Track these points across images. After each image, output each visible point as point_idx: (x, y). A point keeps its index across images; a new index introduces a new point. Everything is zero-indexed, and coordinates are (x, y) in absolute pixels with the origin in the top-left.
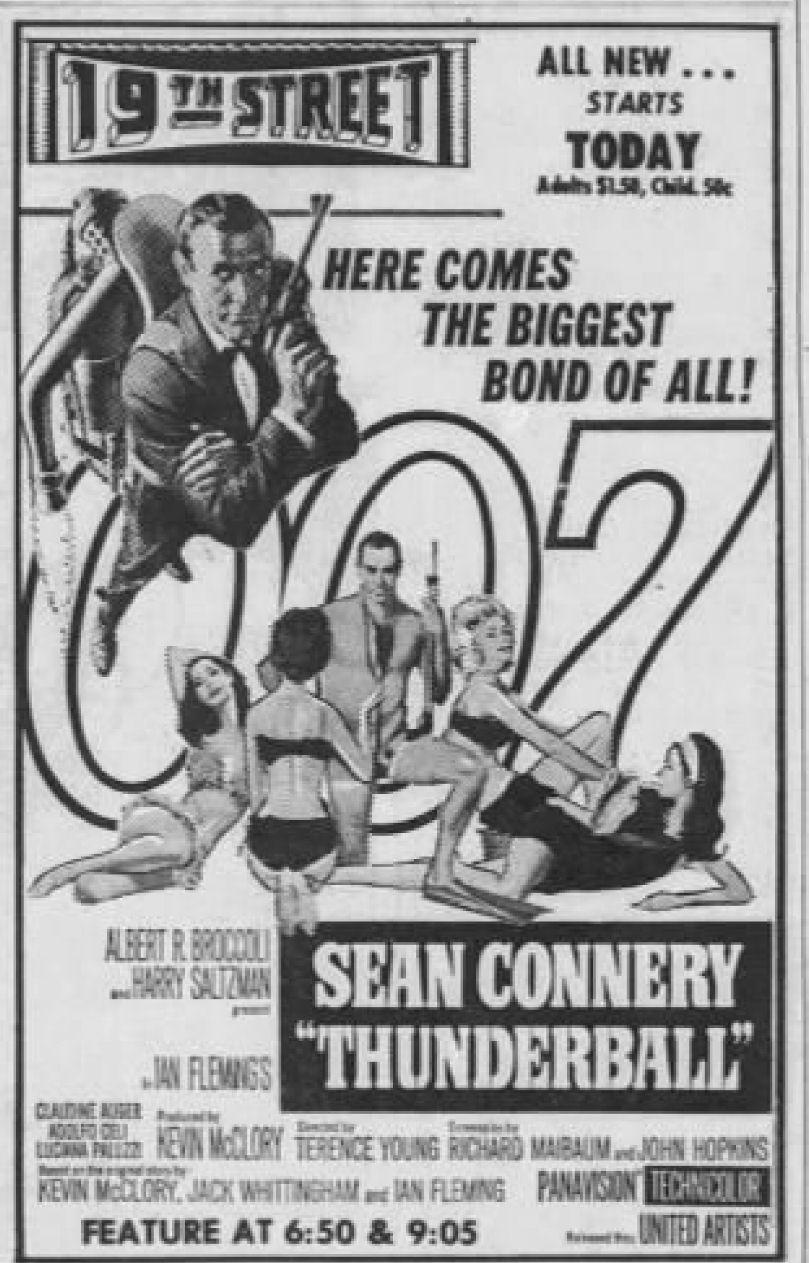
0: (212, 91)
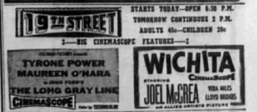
0: (61, 20)
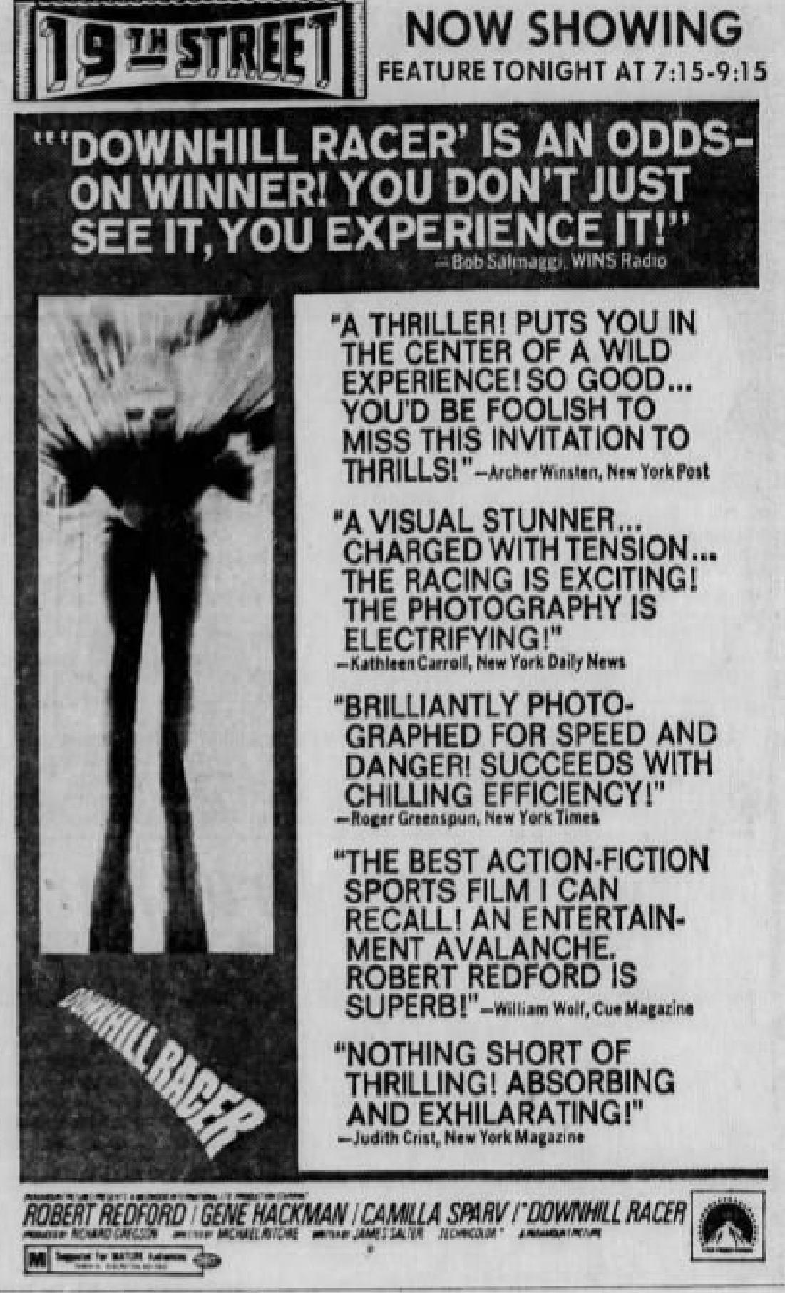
0: (159, 40)
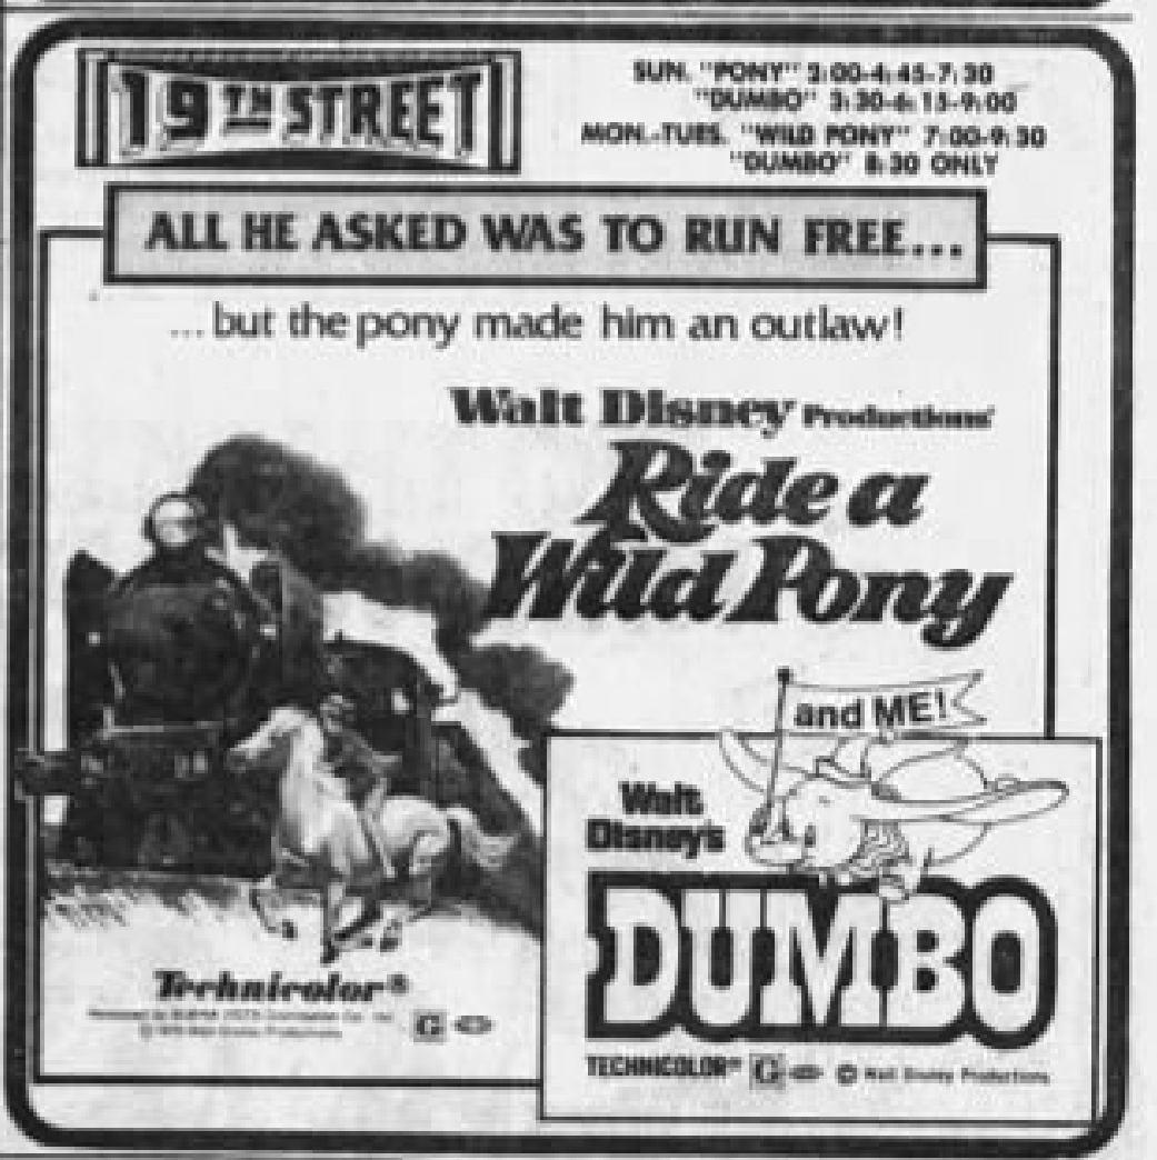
0: (263, 101)
